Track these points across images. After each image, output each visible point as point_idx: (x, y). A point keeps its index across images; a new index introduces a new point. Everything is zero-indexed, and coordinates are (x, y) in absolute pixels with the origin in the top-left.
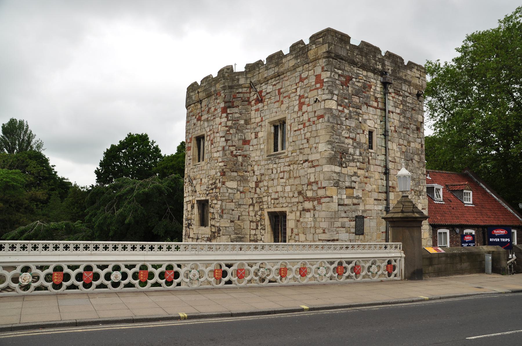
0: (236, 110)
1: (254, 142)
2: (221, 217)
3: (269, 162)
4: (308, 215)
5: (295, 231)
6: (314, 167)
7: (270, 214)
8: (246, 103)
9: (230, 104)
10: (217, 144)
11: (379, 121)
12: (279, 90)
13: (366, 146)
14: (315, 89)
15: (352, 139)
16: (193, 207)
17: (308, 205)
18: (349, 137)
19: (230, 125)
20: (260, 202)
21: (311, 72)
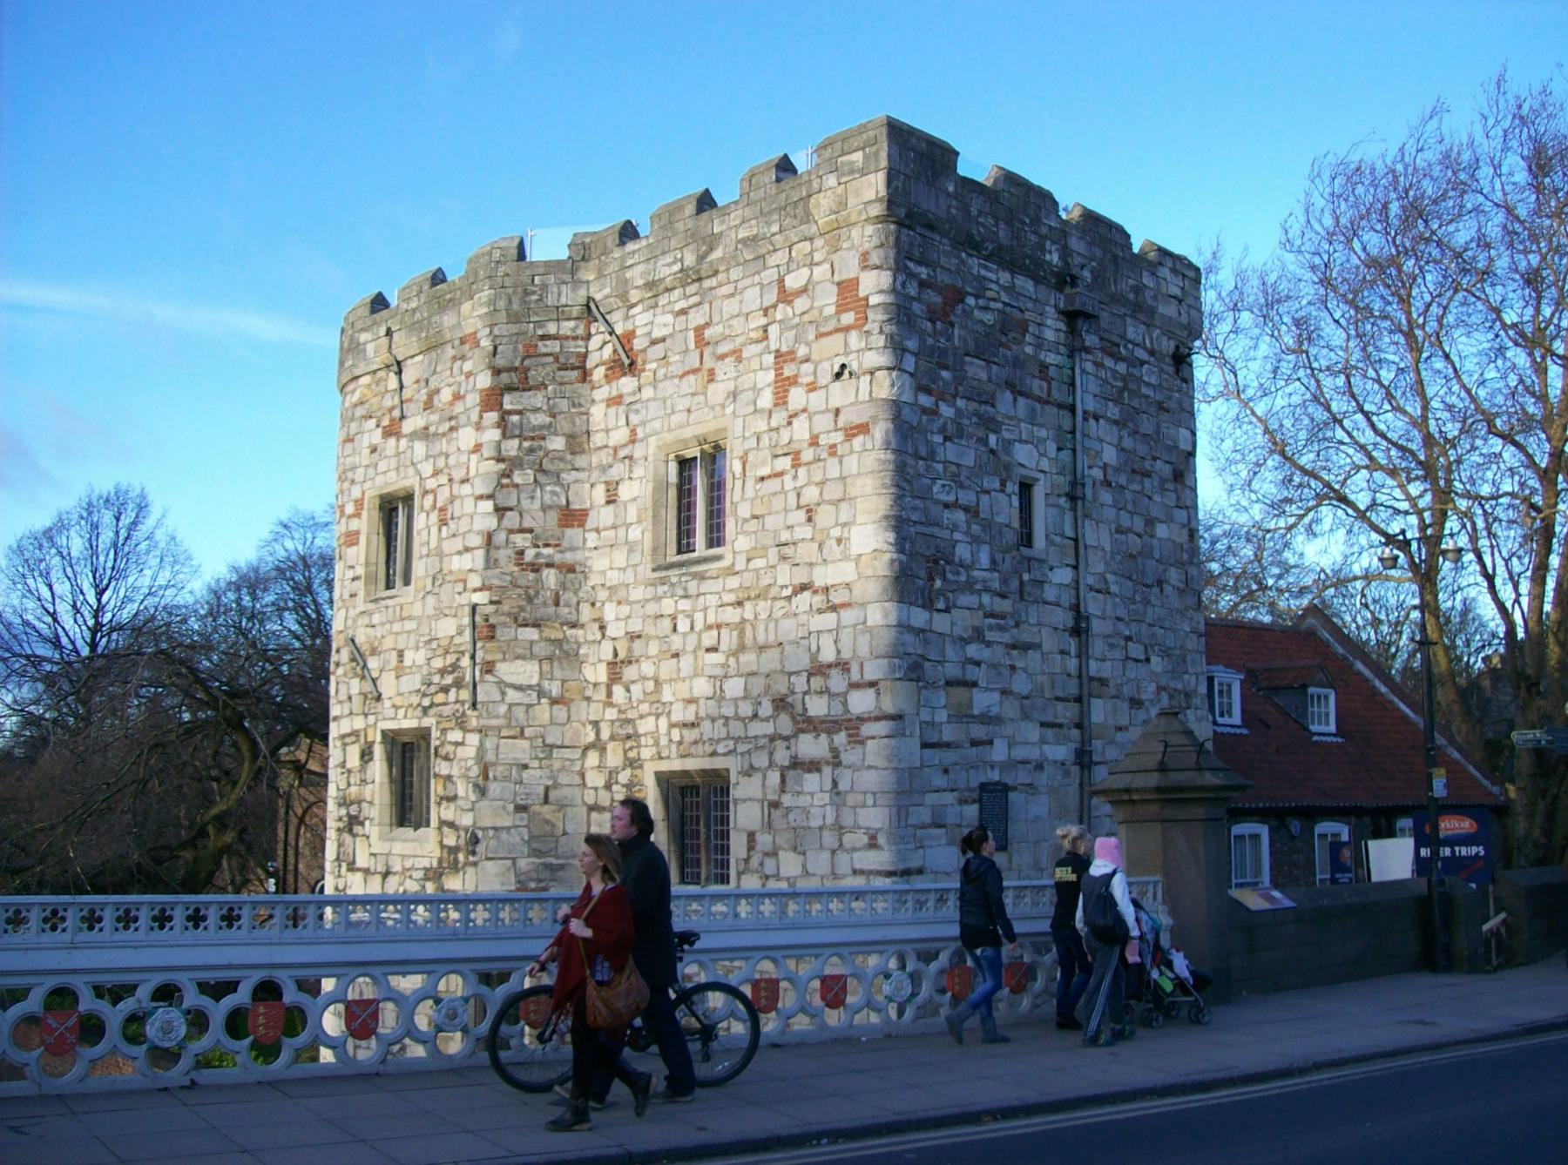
0: (538, 399)
1: (603, 516)
2: (482, 791)
3: (662, 589)
4: (811, 781)
5: (764, 840)
6: (834, 608)
8: (575, 374)
9: (514, 378)
10: (464, 525)
11: (1051, 447)
12: (699, 330)
13: (1010, 537)
14: (837, 330)
15: (966, 510)
16: (366, 755)
17: (811, 746)
18: (954, 505)
19: (514, 453)
20: (629, 737)
21: (821, 272)
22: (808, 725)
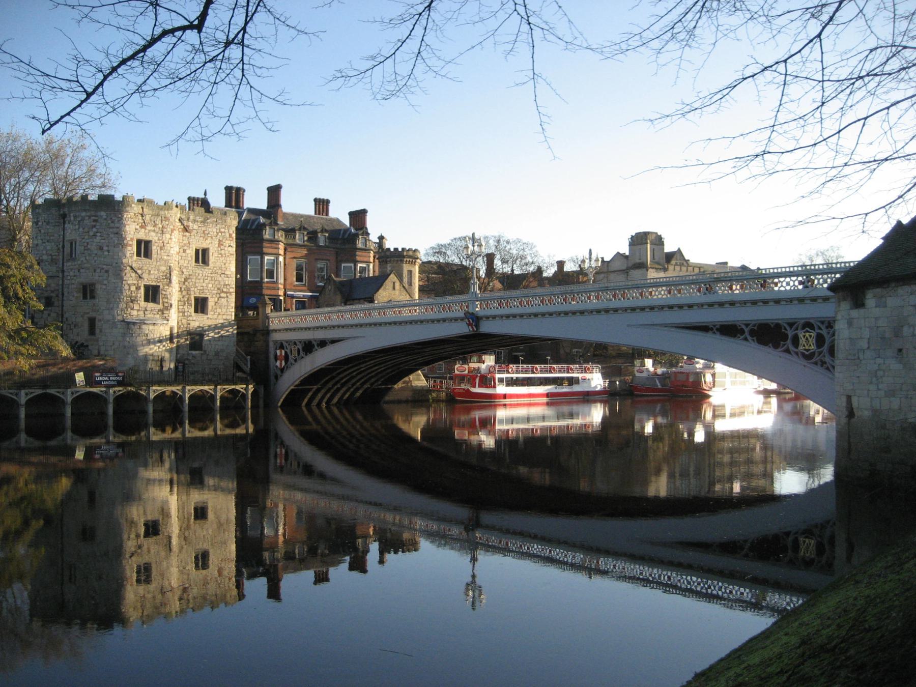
7: (196, 299)
22: (223, 292)
